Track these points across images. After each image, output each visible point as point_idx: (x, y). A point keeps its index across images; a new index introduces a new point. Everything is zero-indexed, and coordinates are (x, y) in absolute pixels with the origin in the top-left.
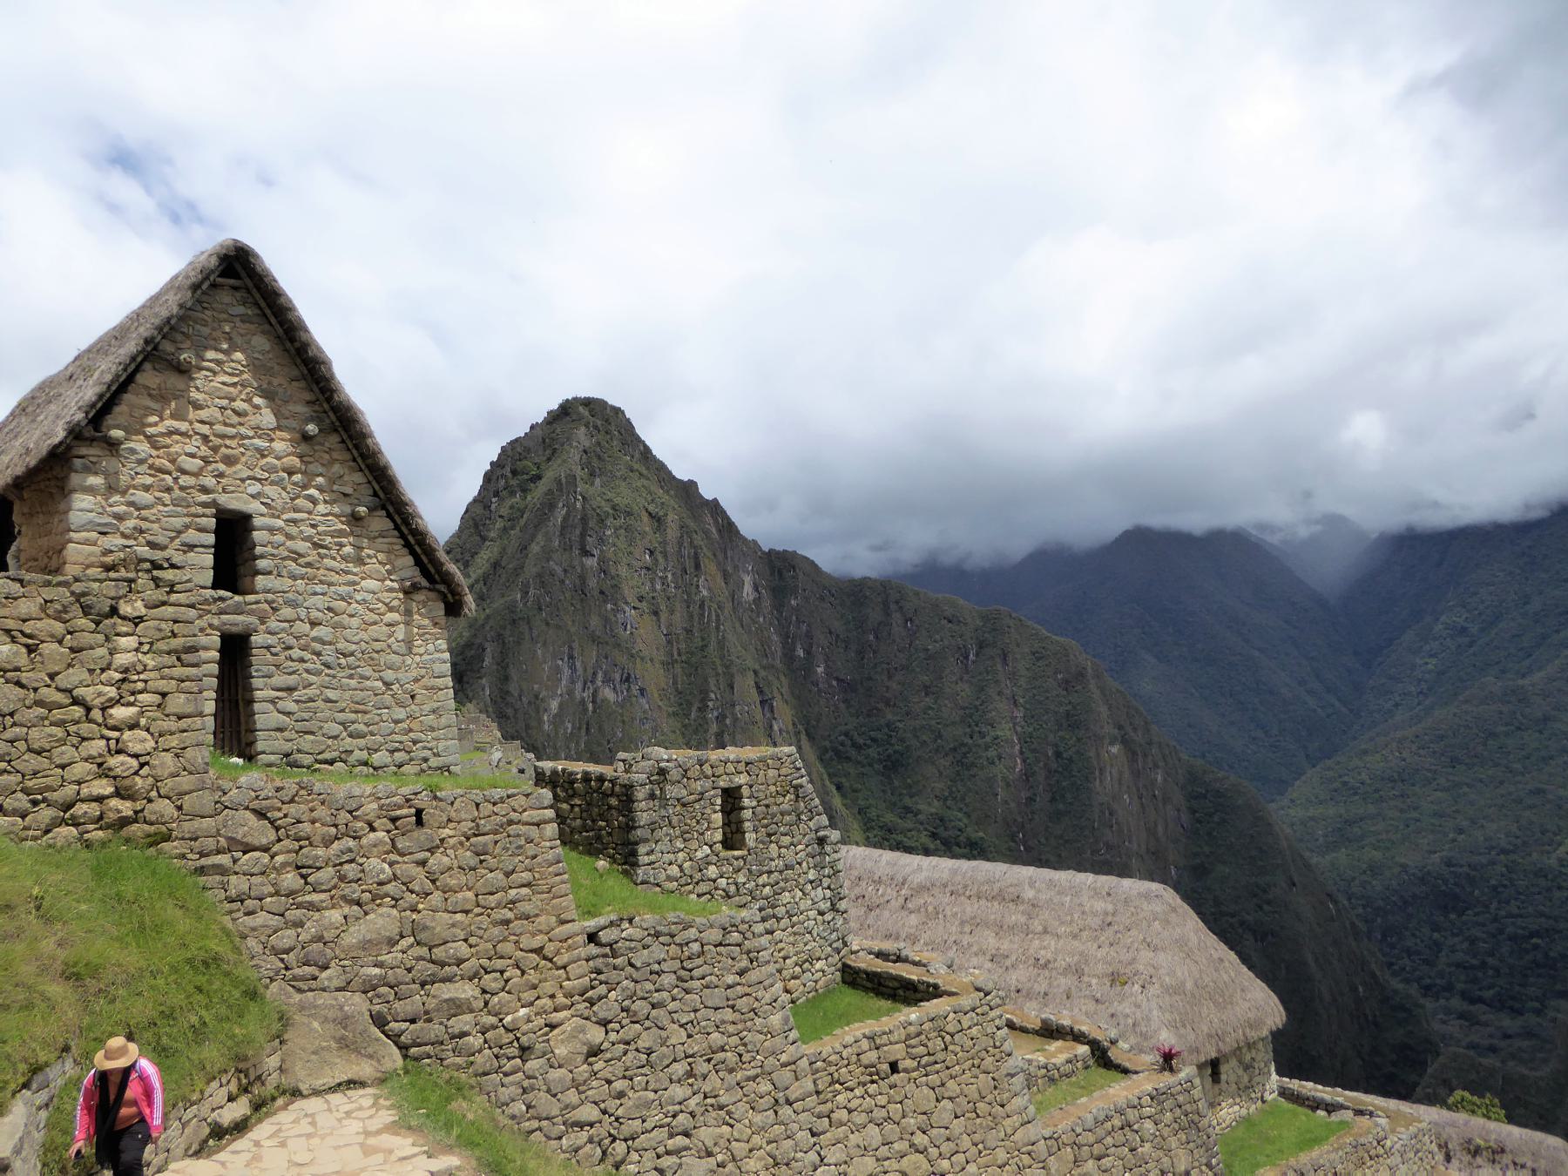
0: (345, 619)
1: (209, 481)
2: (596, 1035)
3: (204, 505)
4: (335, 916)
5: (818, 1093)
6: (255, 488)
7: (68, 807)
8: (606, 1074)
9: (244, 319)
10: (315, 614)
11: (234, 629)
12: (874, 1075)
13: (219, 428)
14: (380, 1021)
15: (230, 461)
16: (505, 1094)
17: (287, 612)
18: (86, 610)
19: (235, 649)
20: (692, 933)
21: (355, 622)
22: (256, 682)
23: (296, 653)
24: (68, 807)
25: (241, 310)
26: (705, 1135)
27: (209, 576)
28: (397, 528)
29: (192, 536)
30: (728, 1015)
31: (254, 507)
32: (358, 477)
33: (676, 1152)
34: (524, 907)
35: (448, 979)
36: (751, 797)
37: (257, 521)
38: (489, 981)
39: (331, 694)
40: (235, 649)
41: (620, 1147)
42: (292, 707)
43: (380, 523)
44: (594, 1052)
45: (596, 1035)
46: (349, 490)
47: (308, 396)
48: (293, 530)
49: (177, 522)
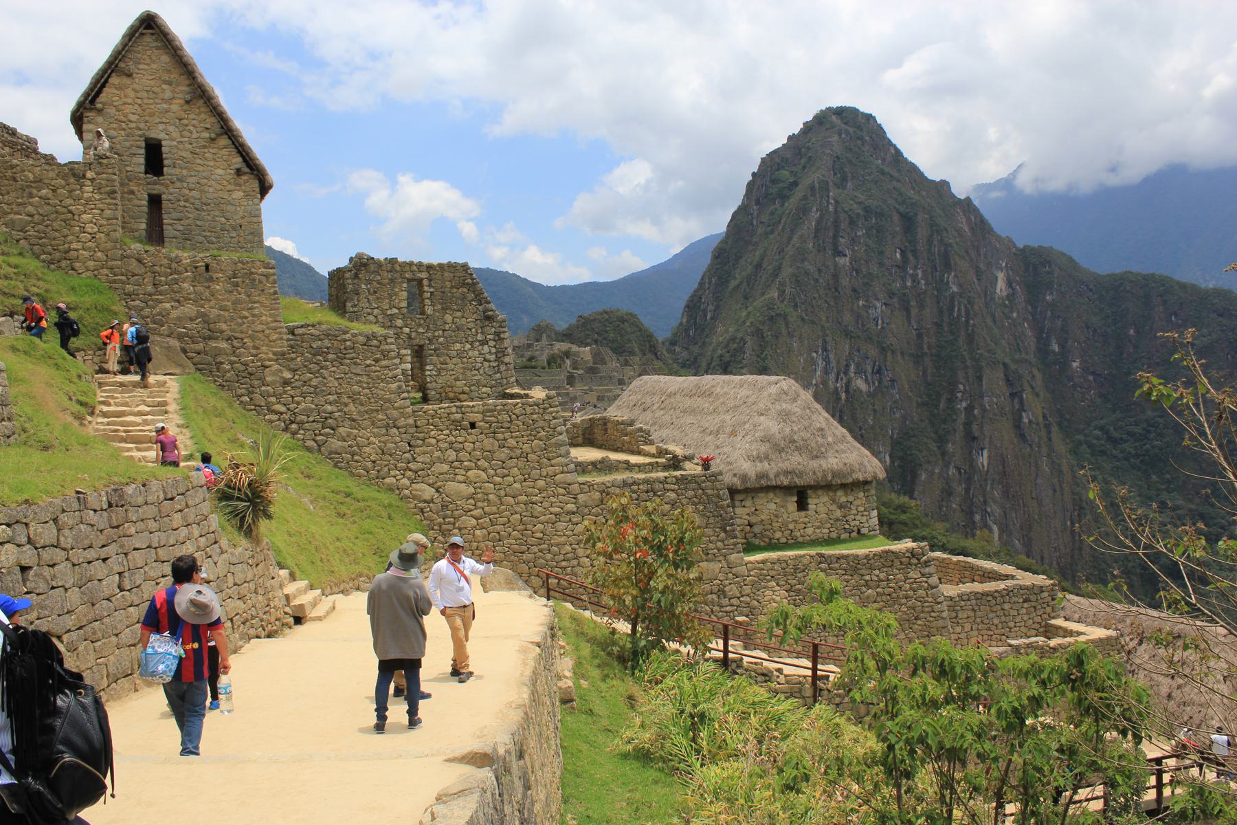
0: (206, 188)
1: (142, 126)
2: (288, 375)
4: (168, 305)
6: (161, 127)
7: (67, 252)
8: (291, 393)
9: (158, 48)
10: (191, 186)
12: (457, 425)
13: (146, 101)
14: (184, 351)
15: (152, 115)
16: (239, 392)
17: (178, 184)
18: (74, 175)
19: (155, 202)
20: (347, 336)
21: (211, 190)
22: (165, 216)
23: (182, 203)
24: (67, 252)
25: (155, 44)
26: (342, 431)
27: (143, 168)
29: (134, 150)
30: (365, 379)
31: (161, 136)
32: (213, 120)
33: (326, 435)
34: (256, 312)
35: (217, 338)
36: (430, 286)
37: (163, 143)
38: (236, 343)
39: (199, 223)
40: (155, 202)
41: (294, 426)
42: (181, 228)
43: (224, 141)
44: (286, 383)
45: (288, 375)
47: (187, 82)
48: (181, 147)
49: (127, 144)
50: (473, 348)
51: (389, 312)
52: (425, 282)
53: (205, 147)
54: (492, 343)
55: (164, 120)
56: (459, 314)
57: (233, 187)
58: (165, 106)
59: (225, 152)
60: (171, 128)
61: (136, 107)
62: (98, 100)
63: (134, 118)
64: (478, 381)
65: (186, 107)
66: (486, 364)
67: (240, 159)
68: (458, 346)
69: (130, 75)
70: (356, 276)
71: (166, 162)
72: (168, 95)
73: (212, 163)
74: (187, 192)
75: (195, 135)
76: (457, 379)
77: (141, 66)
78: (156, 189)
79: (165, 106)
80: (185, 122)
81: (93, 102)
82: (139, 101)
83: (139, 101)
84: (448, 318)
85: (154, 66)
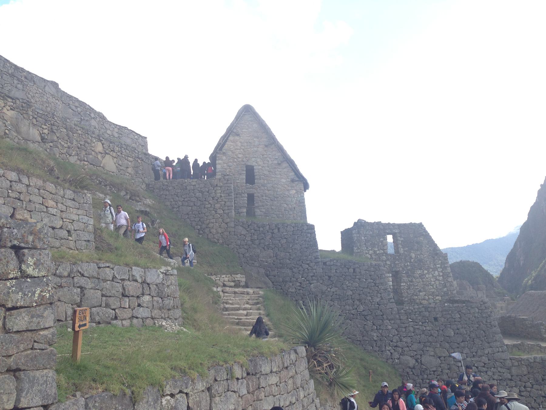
1: (244, 159)
3: (243, 165)
5: (400, 320)
6: (253, 159)
11: (251, 192)
17: (263, 188)
19: (251, 198)
25: (250, 119)
27: (245, 181)
28: (290, 165)
31: (254, 164)
36: (401, 237)
37: (255, 167)
42: (264, 210)
43: (285, 165)
46: (277, 157)
48: (263, 169)
50: (428, 273)
51: (378, 252)
52: (398, 235)
53: (275, 168)
54: (440, 270)
55: (255, 156)
56: (419, 253)
57: (290, 188)
58: (255, 149)
59: (285, 170)
60: (259, 160)
61: (242, 150)
62: (224, 148)
63: (240, 156)
64: (433, 292)
65: (266, 149)
66: (437, 282)
67: (293, 173)
68: (419, 272)
69: (238, 135)
70: (359, 233)
71: (256, 177)
72: (257, 143)
73: (279, 176)
74: (267, 192)
75: (270, 162)
76: (420, 291)
77: (244, 130)
78: (252, 191)
79: (255, 149)
80: (265, 156)
81: (221, 149)
82: (243, 148)
83: (243, 148)
84: (413, 255)
85: (250, 130)
